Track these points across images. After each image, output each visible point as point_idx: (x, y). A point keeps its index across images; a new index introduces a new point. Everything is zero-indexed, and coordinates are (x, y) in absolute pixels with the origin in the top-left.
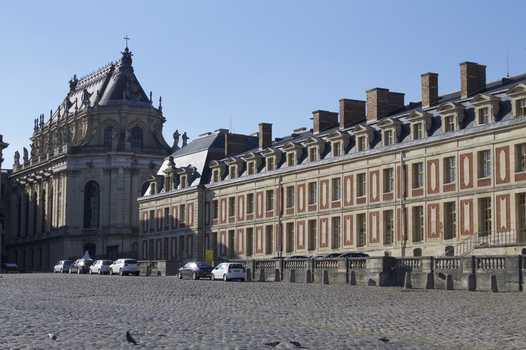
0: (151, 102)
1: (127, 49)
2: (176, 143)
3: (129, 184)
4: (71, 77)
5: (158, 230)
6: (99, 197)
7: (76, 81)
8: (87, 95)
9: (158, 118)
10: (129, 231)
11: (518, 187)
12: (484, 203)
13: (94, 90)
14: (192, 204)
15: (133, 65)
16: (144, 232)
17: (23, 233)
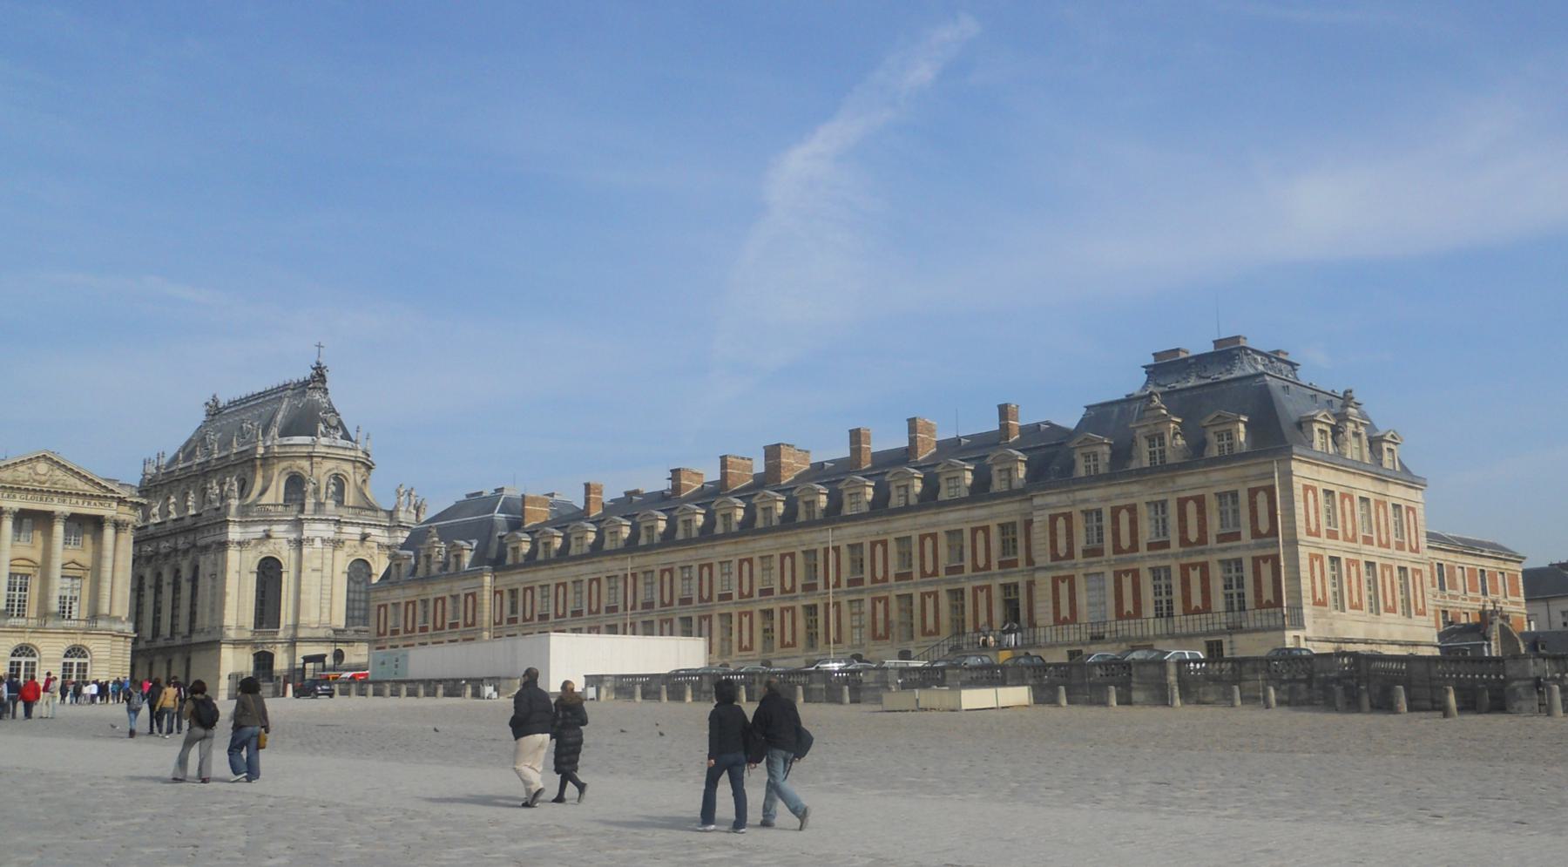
11: (1003, 575)
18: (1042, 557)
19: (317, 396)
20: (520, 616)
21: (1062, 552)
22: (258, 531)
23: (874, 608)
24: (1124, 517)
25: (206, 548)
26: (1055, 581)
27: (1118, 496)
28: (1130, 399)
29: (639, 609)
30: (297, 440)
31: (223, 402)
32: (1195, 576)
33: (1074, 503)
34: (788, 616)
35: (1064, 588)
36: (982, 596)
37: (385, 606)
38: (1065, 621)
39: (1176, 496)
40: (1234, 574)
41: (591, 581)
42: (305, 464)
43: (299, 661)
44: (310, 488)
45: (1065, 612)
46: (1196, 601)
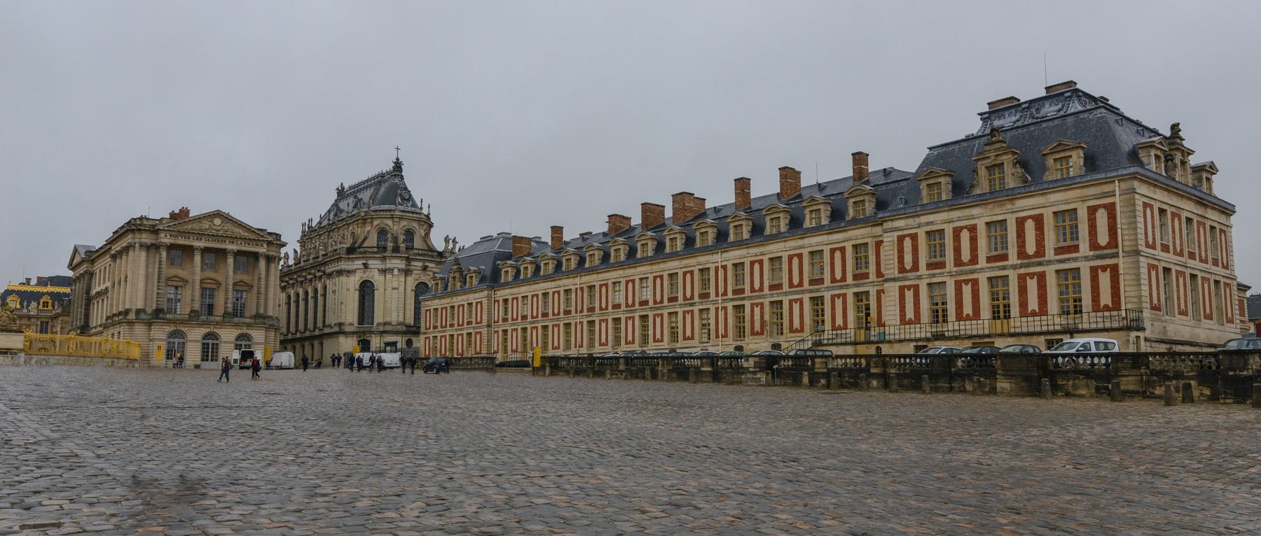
2: (446, 247)
4: (338, 185)
9: (427, 223)
12: (817, 301)
13: (365, 196)
17: (292, 329)
18: (891, 269)
19: (397, 180)
20: (509, 317)
21: (908, 265)
22: (358, 264)
23: (752, 311)
26: (902, 289)
27: (959, 219)
28: (969, 139)
29: (585, 313)
30: (386, 207)
31: (346, 186)
32: (1032, 285)
33: (919, 226)
34: (688, 317)
35: (909, 295)
36: (839, 302)
38: (910, 322)
40: (1070, 281)
42: (389, 222)
45: (910, 314)
46: (1033, 304)
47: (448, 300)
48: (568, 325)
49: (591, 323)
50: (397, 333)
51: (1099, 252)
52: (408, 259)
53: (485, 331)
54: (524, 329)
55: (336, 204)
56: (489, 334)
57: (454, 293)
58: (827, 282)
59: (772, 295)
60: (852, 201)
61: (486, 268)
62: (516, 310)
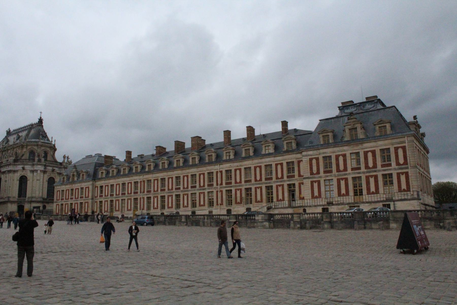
0: (52, 141)
1: (41, 118)
2: (64, 161)
3: (42, 178)
4: (7, 129)
5: (66, 199)
6: (27, 184)
7: (10, 131)
8: (19, 137)
9: (54, 149)
10: (42, 200)
11: (289, 181)
13: (23, 134)
14: (88, 187)
15: (43, 124)
16: (57, 200)
19: (40, 128)
22: (20, 167)
24: (341, 159)
25: (4, 172)
26: (312, 183)
27: (339, 151)
30: (33, 140)
31: (12, 130)
32: (372, 180)
33: (320, 154)
35: (316, 185)
37: (59, 191)
38: (316, 197)
39: (335, 154)
40: (388, 179)
41: (128, 183)
42: (36, 148)
43: (32, 208)
44: (36, 154)
45: (316, 194)
46: (373, 189)
47: (71, 186)
48: (136, 199)
49: (149, 198)
50: (38, 202)
51: (400, 167)
52: (45, 166)
53: (90, 201)
54: (112, 201)
55: (6, 137)
56: (93, 203)
57: (73, 182)
58: (274, 179)
59: (246, 185)
60: (285, 142)
61: (91, 170)
62: (106, 191)
